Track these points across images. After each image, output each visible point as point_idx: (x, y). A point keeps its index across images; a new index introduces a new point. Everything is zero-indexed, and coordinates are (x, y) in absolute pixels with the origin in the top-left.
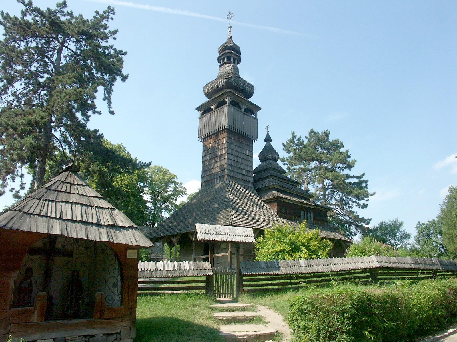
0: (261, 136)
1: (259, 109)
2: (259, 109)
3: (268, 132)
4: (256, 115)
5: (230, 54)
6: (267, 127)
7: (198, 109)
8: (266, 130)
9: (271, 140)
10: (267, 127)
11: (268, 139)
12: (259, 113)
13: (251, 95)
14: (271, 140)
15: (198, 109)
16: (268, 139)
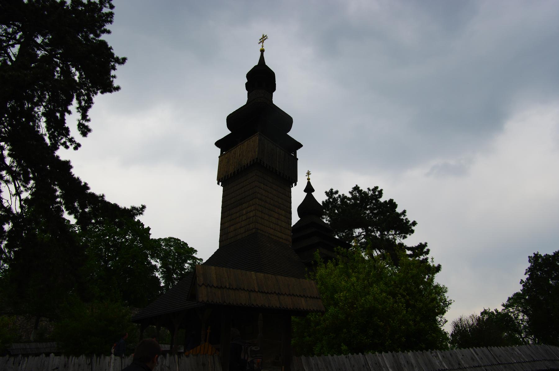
0: (302, 183)
1: (300, 146)
2: (300, 146)
3: (308, 179)
4: (295, 154)
5: (261, 80)
6: (308, 174)
7: (218, 144)
8: (307, 177)
9: (313, 191)
10: (308, 174)
11: (309, 189)
12: (298, 152)
13: (289, 129)
14: (313, 191)
15: (218, 144)
16: (309, 189)
